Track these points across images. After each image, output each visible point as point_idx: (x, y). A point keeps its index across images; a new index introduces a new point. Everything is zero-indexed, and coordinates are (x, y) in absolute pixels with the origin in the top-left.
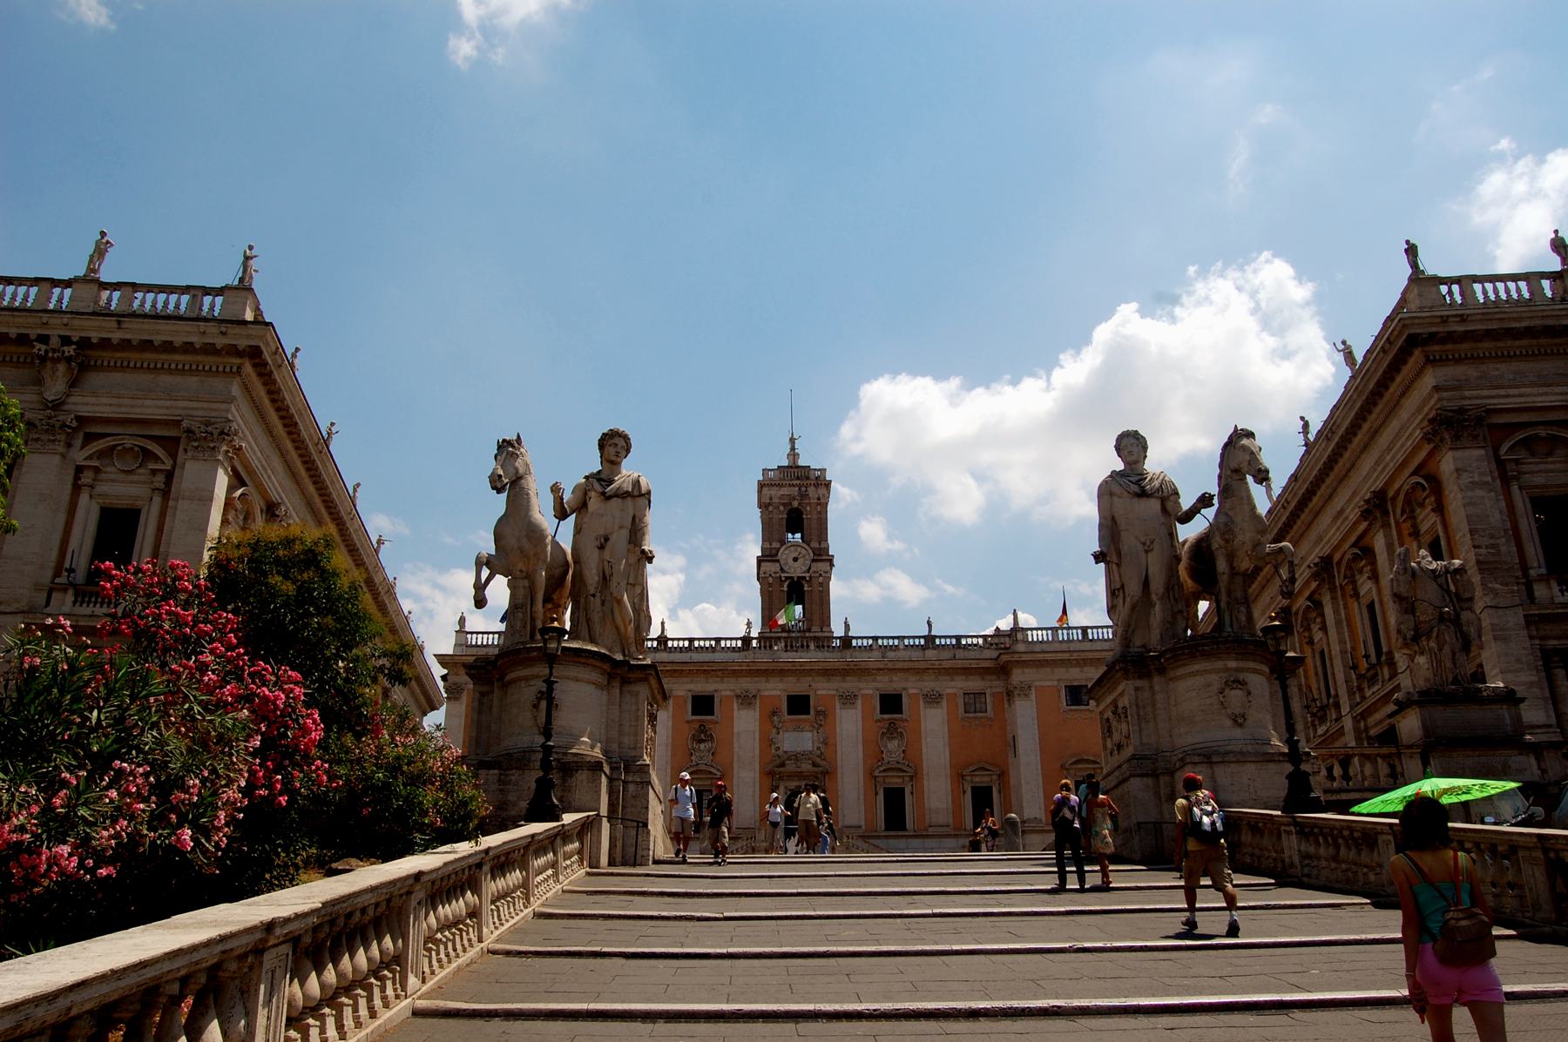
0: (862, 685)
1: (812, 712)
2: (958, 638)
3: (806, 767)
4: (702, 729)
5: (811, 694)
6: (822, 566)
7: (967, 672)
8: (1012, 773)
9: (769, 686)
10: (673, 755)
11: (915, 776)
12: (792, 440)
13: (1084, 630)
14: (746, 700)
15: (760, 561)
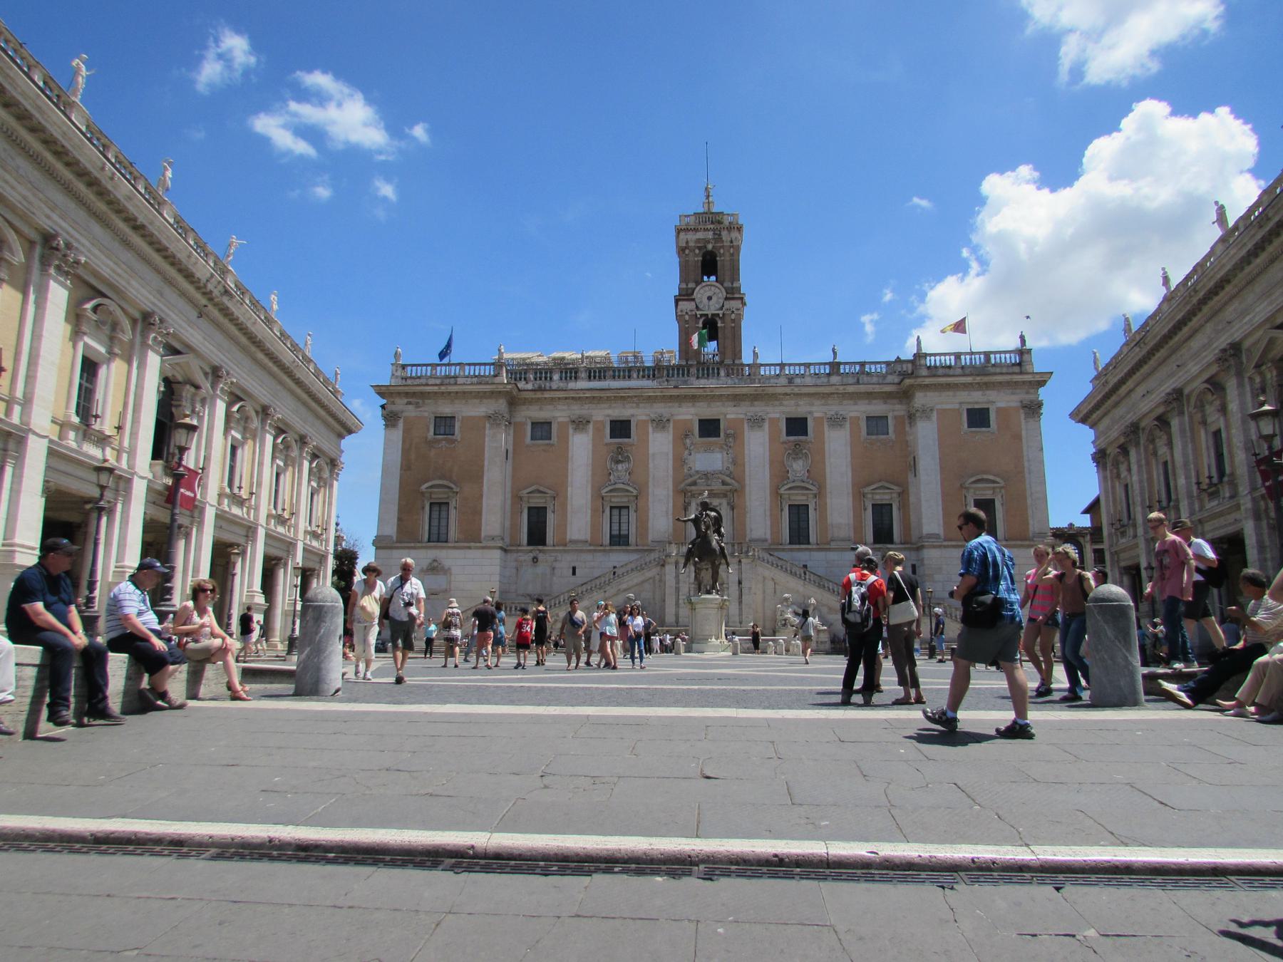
0: (769, 409)
2: (863, 364)
3: (717, 486)
4: (620, 449)
5: (721, 417)
6: (734, 304)
7: (870, 396)
8: (912, 490)
9: (683, 410)
10: (593, 475)
11: (820, 494)
12: (707, 189)
14: (660, 423)
15: (677, 301)
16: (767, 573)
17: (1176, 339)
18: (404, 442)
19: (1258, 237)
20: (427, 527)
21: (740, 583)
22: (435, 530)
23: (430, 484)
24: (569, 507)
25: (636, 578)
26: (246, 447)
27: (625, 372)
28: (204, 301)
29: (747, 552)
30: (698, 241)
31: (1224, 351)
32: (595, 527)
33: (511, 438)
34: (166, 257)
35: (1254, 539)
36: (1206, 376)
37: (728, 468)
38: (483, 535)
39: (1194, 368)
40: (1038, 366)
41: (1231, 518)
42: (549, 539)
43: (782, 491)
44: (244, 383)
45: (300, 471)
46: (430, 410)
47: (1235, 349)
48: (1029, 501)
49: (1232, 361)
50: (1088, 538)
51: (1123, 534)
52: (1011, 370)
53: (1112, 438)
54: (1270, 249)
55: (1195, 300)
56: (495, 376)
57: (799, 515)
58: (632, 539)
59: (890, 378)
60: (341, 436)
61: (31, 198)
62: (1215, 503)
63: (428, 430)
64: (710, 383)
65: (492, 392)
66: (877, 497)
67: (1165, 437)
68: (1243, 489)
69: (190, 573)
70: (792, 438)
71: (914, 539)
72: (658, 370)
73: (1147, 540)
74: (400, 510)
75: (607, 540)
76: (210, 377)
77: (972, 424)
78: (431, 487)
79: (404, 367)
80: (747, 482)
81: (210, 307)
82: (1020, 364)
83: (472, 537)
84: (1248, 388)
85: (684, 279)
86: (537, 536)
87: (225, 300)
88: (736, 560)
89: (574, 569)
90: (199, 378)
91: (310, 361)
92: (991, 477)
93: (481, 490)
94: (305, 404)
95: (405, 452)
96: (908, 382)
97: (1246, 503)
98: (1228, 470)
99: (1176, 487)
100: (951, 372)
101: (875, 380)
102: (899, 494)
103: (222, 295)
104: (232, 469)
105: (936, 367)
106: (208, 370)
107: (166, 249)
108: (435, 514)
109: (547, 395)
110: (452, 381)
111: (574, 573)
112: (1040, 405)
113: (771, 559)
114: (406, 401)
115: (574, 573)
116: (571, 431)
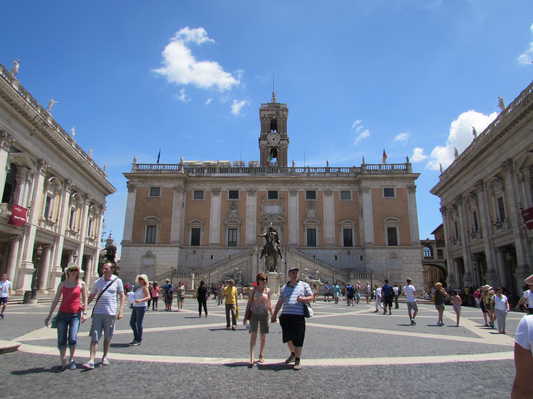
0: (299, 187)
1: (278, 197)
2: (339, 168)
5: (278, 190)
6: (284, 142)
7: (343, 182)
8: (361, 223)
9: (261, 187)
10: (221, 214)
11: (321, 225)
13: (392, 165)
14: (251, 192)
15: (260, 140)
16: (298, 259)
17: (481, 157)
18: (136, 198)
19: (523, 110)
20: (146, 237)
21: (286, 263)
22: (149, 238)
23: (146, 218)
24: (210, 229)
25: (239, 261)
26: (56, 198)
27: (236, 170)
28: (34, 128)
29: (289, 250)
30: (269, 115)
31: (504, 162)
32: (222, 238)
33: (185, 198)
34: (12, 105)
35: (520, 247)
36: (495, 174)
37: (281, 213)
38: (171, 240)
39: (489, 170)
40: (414, 170)
41: (507, 237)
42: (201, 243)
43: (304, 223)
44: (54, 167)
45: (84, 211)
46: (148, 185)
47: (510, 161)
48: (411, 229)
49: (508, 167)
50: (435, 245)
51: (455, 244)
52: (403, 172)
53: (449, 201)
54: (528, 116)
55: (491, 140)
56: (179, 170)
57: (312, 234)
58: (238, 243)
59: (351, 175)
60: (106, 195)
62: (500, 230)
63: (148, 192)
64: (274, 175)
65: (177, 177)
66: (346, 226)
67: (474, 201)
68: (515, 224)
69: (21, 258)
70: (309, 200)
71: (362, 244)
72: (251, 169)
73: (466, 247)
74: (134, 229)
75: (227, 244)
76: (37, 165)
77: (386, 195)
78: (148, 219)
79: (138, 165)
80: (289, 219)
81: (37, 131)
82: (406, 170)
83: (166, 242)
84: (516, 179)
85: (263, 130)
86: (196, 241)
87: (45, 127)
88: (284, 253)
89: (212, 256)
90: (31, 165)
91: (91, 160)
92: (395, 218)
93: (171, 220)
94: (88, 180)
95: (137, 203)
96: (359, 176)
97: (516, 231)
98: (506, 216)
99: (480, 223)
100: (377, 173)
101: (345, 175)
102: (355, 225)
103: (43, 125)
104: (47, 208)
105: (371, 170)
106: (36, 161)
107: (12, 100)
108: (150, 231)
109: (202, 179)
110: (159, 172)
111: (212, 258)
112: (415, 187)
113: (299, 253)
114: (138, 180)
115: (212, 258)
116: (212, 195)
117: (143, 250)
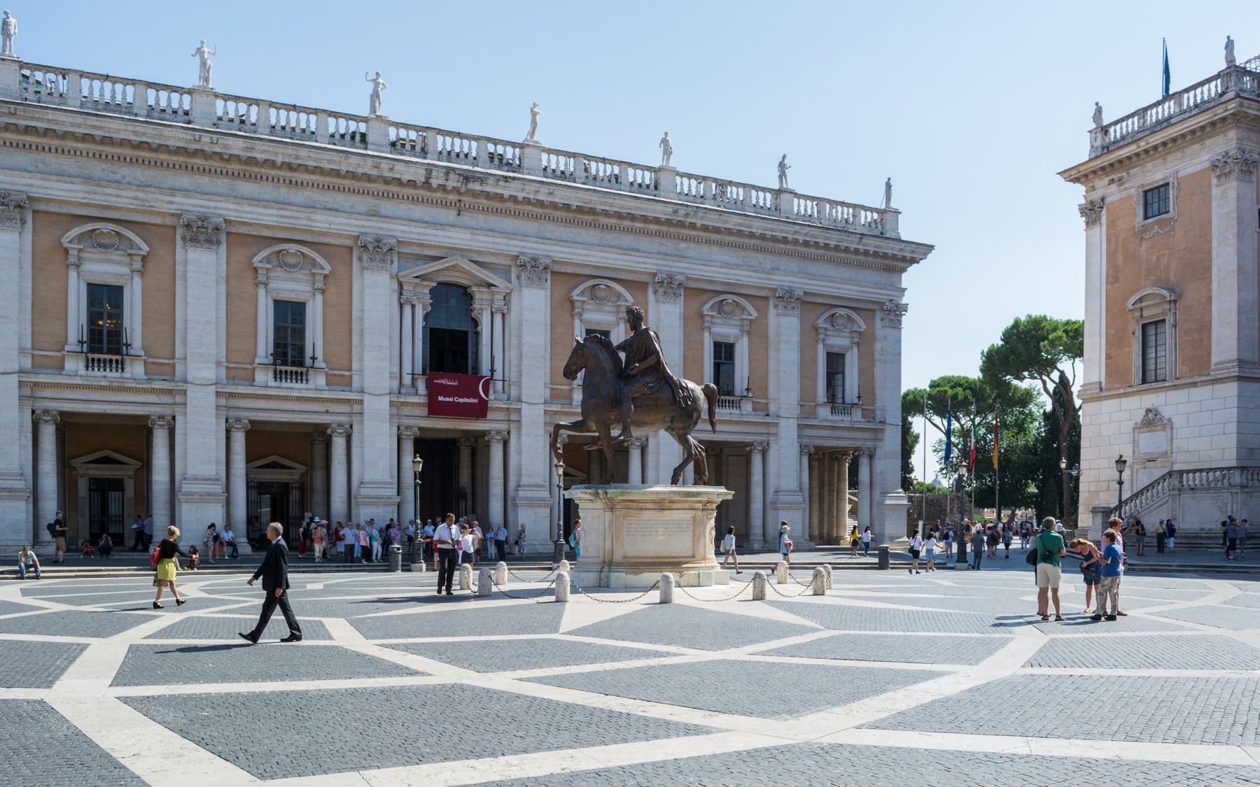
61: (141, 195)
78: (1141, 300)
83: (1198, 369)
93: (1210, 290)
95: (1111, 256)
110: (1165, 125)
114: (1107, 179)
117: (1136, 406)
